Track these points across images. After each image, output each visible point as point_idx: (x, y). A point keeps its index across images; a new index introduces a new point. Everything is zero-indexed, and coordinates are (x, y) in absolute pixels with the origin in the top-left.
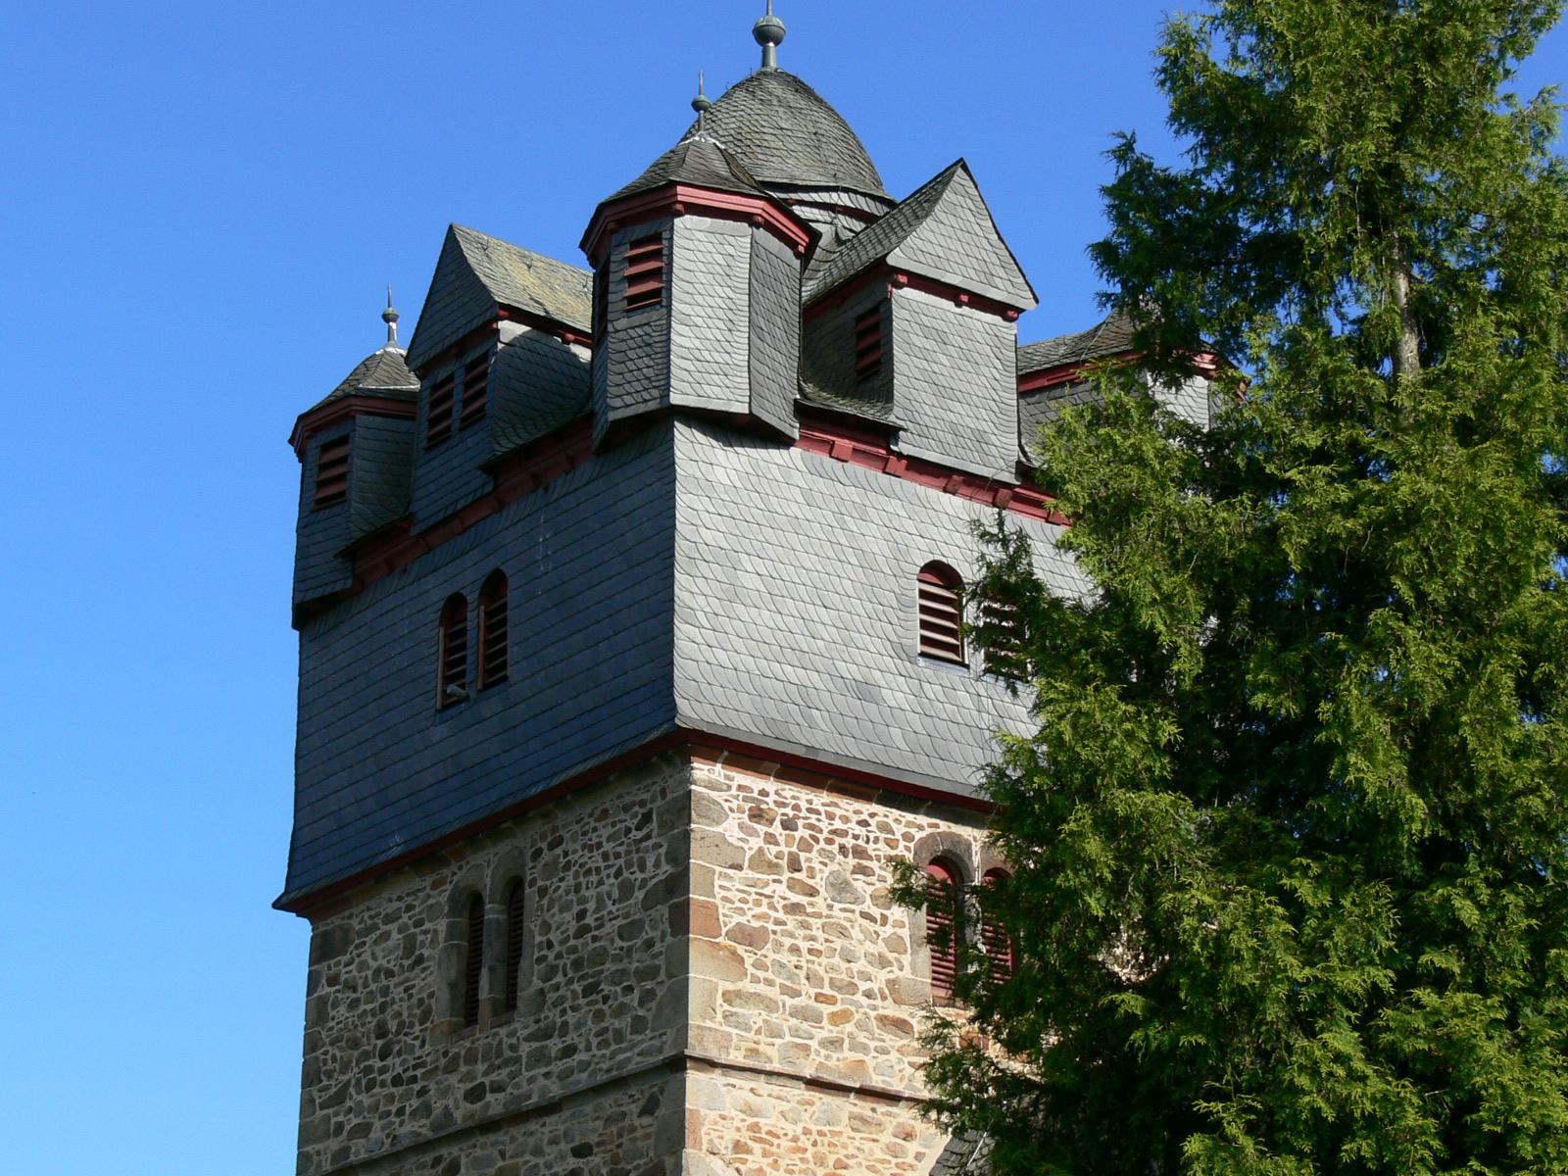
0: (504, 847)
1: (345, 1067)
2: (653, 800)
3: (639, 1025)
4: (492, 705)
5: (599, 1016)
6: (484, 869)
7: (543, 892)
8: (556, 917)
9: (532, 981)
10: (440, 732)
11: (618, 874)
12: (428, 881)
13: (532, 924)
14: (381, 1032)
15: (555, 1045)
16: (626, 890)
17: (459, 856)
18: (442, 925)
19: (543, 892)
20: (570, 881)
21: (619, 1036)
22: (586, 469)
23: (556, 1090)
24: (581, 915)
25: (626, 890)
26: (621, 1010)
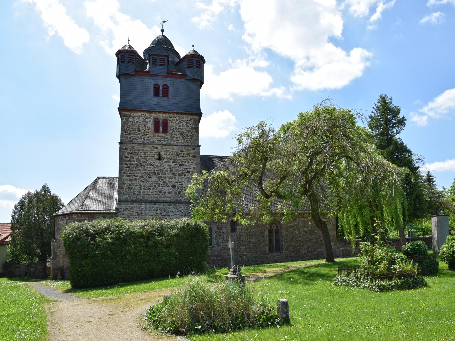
0: (164, 115)
1: (131, 131)
3: (190, 141)
4: (165, 99)
5: (183, 138)
6: (161, 116)
7: (172, 122)
8: (174, 125)
9: (170, 131)
10: (154, 99)
12: (148, 114)
13: (170, 125)
14: (139, 129)
15: (175, 139)
16: (187, 126)
18: (152, 120)
19: (172, 122)
20: (177, 122)
21: (187, 141)
22: (183, 80)
23: (176, 144)
24: (180, 127)
25: (187, 126)
26: (187, 138)
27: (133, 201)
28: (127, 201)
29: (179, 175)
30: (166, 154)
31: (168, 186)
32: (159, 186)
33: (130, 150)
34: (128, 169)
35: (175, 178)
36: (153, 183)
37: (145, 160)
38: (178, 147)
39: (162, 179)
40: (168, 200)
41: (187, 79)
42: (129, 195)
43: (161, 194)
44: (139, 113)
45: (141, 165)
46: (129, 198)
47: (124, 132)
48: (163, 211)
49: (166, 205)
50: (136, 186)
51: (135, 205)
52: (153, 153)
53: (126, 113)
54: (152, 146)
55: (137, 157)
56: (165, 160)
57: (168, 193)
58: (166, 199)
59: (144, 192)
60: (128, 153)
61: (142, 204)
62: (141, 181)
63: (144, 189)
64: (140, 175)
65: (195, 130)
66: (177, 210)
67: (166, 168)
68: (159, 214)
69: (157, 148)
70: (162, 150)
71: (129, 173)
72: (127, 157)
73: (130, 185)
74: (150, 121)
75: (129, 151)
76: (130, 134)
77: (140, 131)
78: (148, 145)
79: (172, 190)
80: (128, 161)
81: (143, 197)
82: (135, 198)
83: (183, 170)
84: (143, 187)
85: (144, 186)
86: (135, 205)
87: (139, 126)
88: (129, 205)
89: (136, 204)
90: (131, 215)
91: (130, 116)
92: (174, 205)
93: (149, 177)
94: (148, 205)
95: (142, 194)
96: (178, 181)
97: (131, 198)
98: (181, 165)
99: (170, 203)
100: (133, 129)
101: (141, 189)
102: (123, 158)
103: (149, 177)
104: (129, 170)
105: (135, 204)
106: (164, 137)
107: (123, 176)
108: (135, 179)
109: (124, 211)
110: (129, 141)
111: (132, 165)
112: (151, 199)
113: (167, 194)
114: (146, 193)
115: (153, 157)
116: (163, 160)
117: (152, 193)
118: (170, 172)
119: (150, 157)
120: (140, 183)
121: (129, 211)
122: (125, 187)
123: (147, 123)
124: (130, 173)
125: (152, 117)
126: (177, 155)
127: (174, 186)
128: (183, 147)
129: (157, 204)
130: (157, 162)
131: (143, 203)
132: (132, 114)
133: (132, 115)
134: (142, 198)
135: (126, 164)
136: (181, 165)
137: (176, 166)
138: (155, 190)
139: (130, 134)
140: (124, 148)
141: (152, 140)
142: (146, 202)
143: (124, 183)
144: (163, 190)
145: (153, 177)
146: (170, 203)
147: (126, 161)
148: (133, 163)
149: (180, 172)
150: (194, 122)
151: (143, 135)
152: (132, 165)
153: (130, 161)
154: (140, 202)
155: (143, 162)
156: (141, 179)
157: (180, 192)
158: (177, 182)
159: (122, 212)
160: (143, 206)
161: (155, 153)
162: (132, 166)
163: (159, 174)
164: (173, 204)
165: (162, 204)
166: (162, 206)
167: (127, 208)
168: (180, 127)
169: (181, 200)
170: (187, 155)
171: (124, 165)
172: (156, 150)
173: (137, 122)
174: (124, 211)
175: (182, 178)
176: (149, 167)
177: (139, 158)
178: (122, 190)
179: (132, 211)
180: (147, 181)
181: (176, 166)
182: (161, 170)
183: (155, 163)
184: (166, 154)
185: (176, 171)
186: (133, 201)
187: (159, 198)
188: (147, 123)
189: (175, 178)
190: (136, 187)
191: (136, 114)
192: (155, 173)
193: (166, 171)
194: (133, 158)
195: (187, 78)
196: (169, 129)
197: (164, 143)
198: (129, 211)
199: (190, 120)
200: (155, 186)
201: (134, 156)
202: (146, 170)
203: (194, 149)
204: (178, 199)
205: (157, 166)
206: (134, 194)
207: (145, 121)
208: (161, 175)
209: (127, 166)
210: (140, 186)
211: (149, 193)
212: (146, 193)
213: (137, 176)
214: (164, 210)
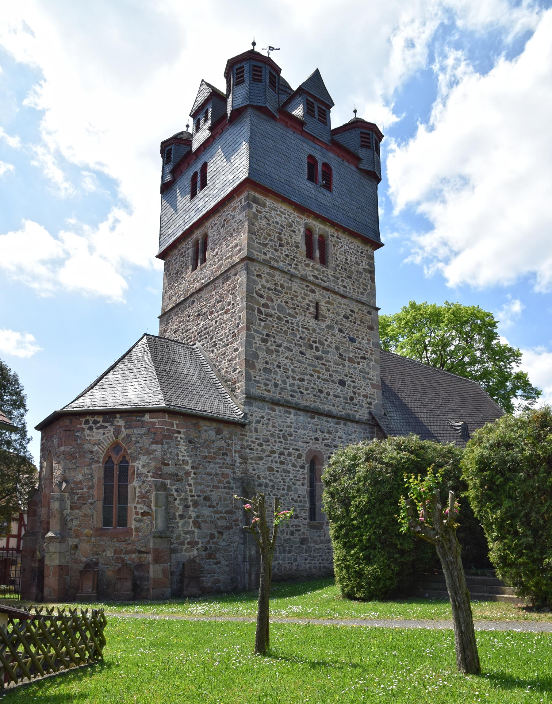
1: (266, 239)
2: (364, 250)
6: (318, 227)
7: (334, 246)
11: (356, 258)
14: (280, 239)
17: (308, 217)
27: (276, 403)
28: (262, 399)
29: (351, 360)
30: (329, 310)
31: (332, 381)
32: (319, 378)
33: (267, 281)
34: (263, 323)
35: (344, 366)
36: (309, 368)
37: (292, 312)
38: (346, 301)
39: (324, 362)
40: (334, 410)
41: (360, 170)
42: (266, 385)
43: (322, 395)
44: (280, 205)
45: (287, 321)
46: (265, 393)
47: (254, 237)
48: (327, 436)
49: (331, 424)
50: (279, 367)
51: (277, 413)
52: (307, 301)
53: (257, 195)
54: (306, 284)
55: (279, 300)
56: (328, 322)
57: (335, 396)
58: (331, 408)
59: (293, 384)
60: (263, 286)
61: (290, 413)
62: (287, 358)
63: (293, 378)
64: (285, 344)
65: (369, 275)
66: (350, 437)
67: (329, 340)
68: (321, 440)
69: (313, 291)
70: (321, 298)
71: (265, 333)
72: (262, 296)
73: (267, 363)
74: (299, 230)
75: (264, 281)
76: (265, 245)
77: (281, 245)
78: (298, 280)
79: (339, 389)
80: (263, 305)
81: (292, 396)
82: (277, 396)
83: (355, 352)
84: (290, 373)
85: (293, 371)
86: (277, 413)
87: (280, 233)
88: (267, 411)
89: (280, 412)
90: (272, 435)
91: (264, 205)
92: (345, 424)
93: (301, 353)
94: (302, 418)
95: (289, 388)
96: (349, 372)
97: (271, 394)
98: (352, 340)
99: (338, 418)
100: (270, 235)
101: (288, 377)
102: (255, 295)
103: (301, 353)
104: (264, 327)
105: (277, 408)
106: (323, 272)
107: (254, 338)
108: (277, 351)
109: (258, 422)
110: (263, 260)
111: (271, 316)
112: (306, 403)
113: (331, 397)
114: (296, 388)
115: (307, 309)
116: (324, 321)
117: (307, 389)
118: (334, 351)
119: (301, 306)
120: (286, 361)
121: (267, 424)
122: (258, 366)
123: (294, 231)
124: (268, 335)
125: (303, 223)
126: (346, 317)
127: (342, 383)
128: (355, 303)
129: (316, 416)
130: (313, 323)
131: (292, 411)
132: (269, 202)
133: (268, 204)
134: (290, 398)
135: (260, 312)
136: (352, 340)
137: (344, 340)
138: (312, 385)
139: (265, 245)
140: (256, 273)
141: (303, 273)
142: (298, 408)
143: (256, 356)
144: (326, 387)
145: (309, 354)
146: (338, 418)
147: (258, 303)
148: (273, 312)
149: (351, 355)
150: (367, 258)
151: (287, 255)
152: (271, 316)
153: (265, 305)
154: (287, 405)
155: (289, 315)
156: (288, 354)
157: (352, 399)
158: (346, 376)
159: (254, 425)
160: (292, 416)
161: (310, 301)
162: (271, 319)
163: (317, 349)
164: (342, 422)
165: (325, 418)
166: (323, 422)
167: (263, 417)
168: (346, 259)
169: (354, 416)
170: (361, 322)
171: (256, 313)
172: (312, 295)
173: (277, 223)
174: (258, 422)
175: (355, 368)
176: (300, 329)
177: (284, 304)
178: (251, 372)
179: (273, 426)
180: (299, 361)
181: (344, 340)
182: (322, 344)
183: (311, 324)
184: (329, 310)
185: (345, 351)
186: (276, 403)
187: (318, 405)
188: (294, 231)
189: (344, 366)
190: (278, 370)
191: (276, 204)
192: (311, 347)
193: (329, 346)
194: (272, 301)
195: (361, 166)
196: (330, 259)
197: (324, 284)
198: (267, 424)
199: (362, 253)
200: (311, 375)
201: (273, 296)
202: (295, 335)
203: (369, 313)
204: (350, 412)
205: (314, 330)
206: (276, 385)
207: (291, 226)
208: (320, 353)
209: (262, 317)
210: (286, 370)
211: (301, 390)
212: (296, 388)
213: (280, 346)
214: (329, 432)
